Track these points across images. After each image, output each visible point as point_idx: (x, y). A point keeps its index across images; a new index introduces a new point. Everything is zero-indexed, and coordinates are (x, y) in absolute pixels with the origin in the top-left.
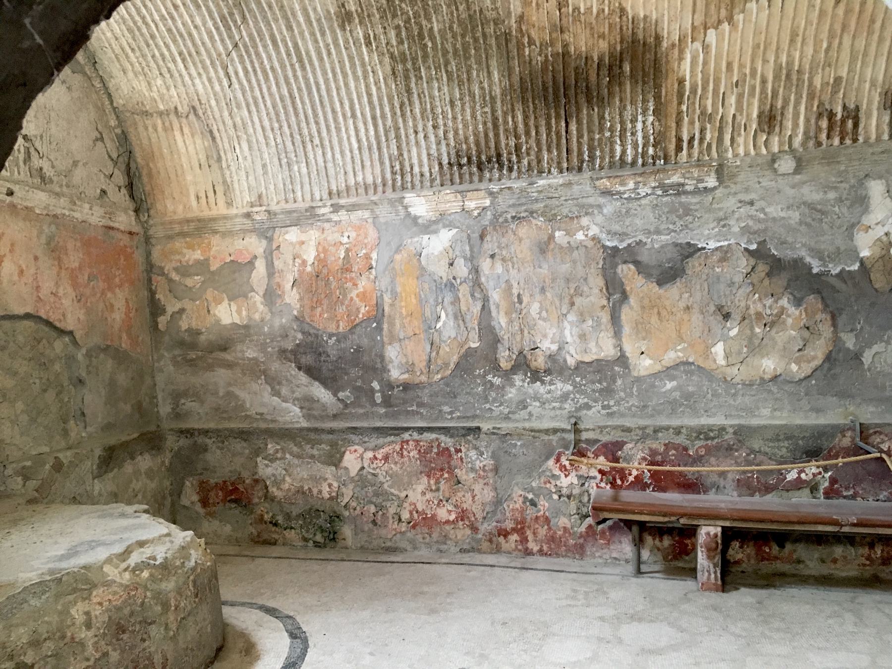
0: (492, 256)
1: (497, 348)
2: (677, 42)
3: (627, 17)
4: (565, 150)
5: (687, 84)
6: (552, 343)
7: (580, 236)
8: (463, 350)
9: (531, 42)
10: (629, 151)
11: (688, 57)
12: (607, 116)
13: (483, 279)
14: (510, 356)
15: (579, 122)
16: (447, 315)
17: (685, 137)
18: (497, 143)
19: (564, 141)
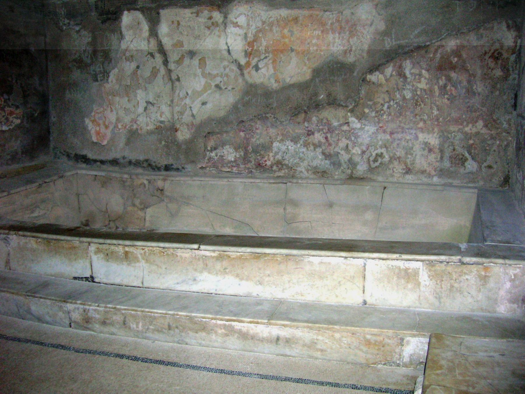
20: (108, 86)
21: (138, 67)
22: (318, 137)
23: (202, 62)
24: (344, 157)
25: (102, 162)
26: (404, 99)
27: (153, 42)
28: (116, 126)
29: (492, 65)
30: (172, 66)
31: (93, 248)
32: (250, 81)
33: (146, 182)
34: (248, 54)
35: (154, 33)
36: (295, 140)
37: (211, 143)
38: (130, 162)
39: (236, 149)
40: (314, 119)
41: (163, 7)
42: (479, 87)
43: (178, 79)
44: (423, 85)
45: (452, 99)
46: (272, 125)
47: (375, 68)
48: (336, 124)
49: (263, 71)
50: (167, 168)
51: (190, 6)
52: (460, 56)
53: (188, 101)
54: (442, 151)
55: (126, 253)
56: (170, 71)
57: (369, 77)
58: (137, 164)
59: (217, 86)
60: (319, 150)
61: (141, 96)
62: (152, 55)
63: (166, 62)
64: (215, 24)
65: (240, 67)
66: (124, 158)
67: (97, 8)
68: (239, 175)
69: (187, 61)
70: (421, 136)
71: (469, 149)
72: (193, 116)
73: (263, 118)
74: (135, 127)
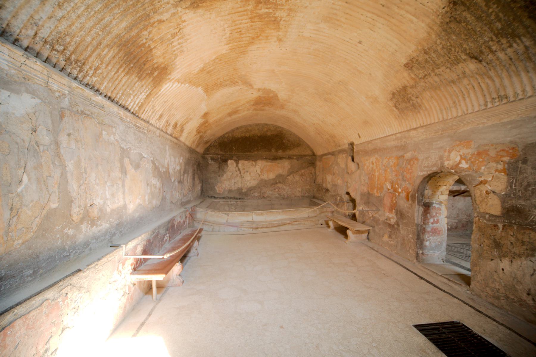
0: (69, 135)
1: (71, 206)
2: (171, 79)
3: (174, 60)
4: (114, 87)
5: (160, 93)
6: (101, 199)
7: (112, 137)
8: (44, 212)
9: (150, 33)
10: (132, 104)
11: (168, 85)
12: (137, 85)
13: (62, 151)
14: (79, 212)
15: (128, 79)
16: (29, 180)
17: (146, 110)
18: (90, 56)
19: (117, 82)
20: (223, 178)
21: (232, 174)
22: (277, 190)
23: (250, 174)
24: (282, 194)
25: (220, 198)
26: (294, 181)
27: (237, 168)
28: (225, 188)
29: (310, 175)
30: (242, 174)
31: (253, 213)
32: (261, 178)
33: (235, 202)
34: (261, 172)
35: (237, 166)
36: (272, 191)
37: (252, 192)
38: (229, 198)
39: (258, 193)
40: (276, 186)
41: (240, 160)
42: (308, 179)
43: (244, 177)
44: (298, 179)
45: (303, 182)
46: (267, 188)
47: (288, 175)
48: (280, 187)
49: (265, 176)
50: (240, 199)
51: (247, 160)
52: (304, 173)
53: (246, 182)
54: (302, 192)
55: (262, 214)
56: (241, 175)
57: (287, 177)
58: (231, 198)
59: (254, 179)
60: (277, 193)
61: (233, 181)
62: (237, 171)
63: (240, 173)
64: (253, 165)
65: (259, 175)
66: (227, 197)
67: (221, 158)
68: (258, 199)
69: (246, 173)
70: (298, 189)
71: (307, 191)
72: (247, 186)
73: (264, 186)
74: (231, 189)
